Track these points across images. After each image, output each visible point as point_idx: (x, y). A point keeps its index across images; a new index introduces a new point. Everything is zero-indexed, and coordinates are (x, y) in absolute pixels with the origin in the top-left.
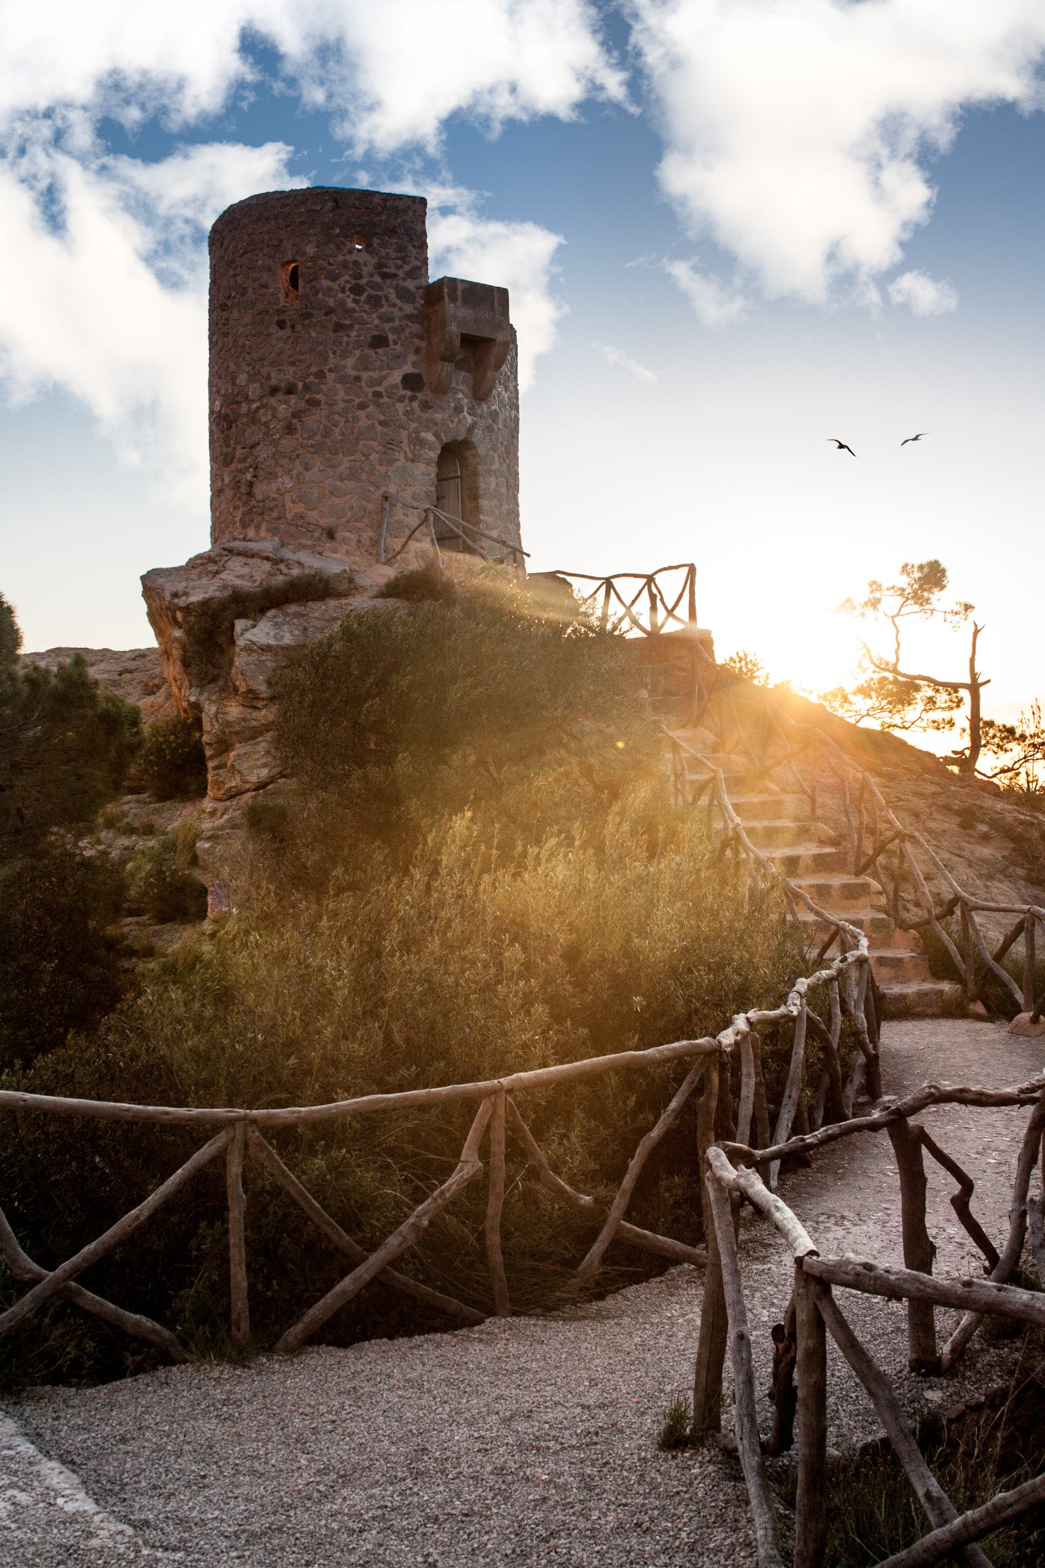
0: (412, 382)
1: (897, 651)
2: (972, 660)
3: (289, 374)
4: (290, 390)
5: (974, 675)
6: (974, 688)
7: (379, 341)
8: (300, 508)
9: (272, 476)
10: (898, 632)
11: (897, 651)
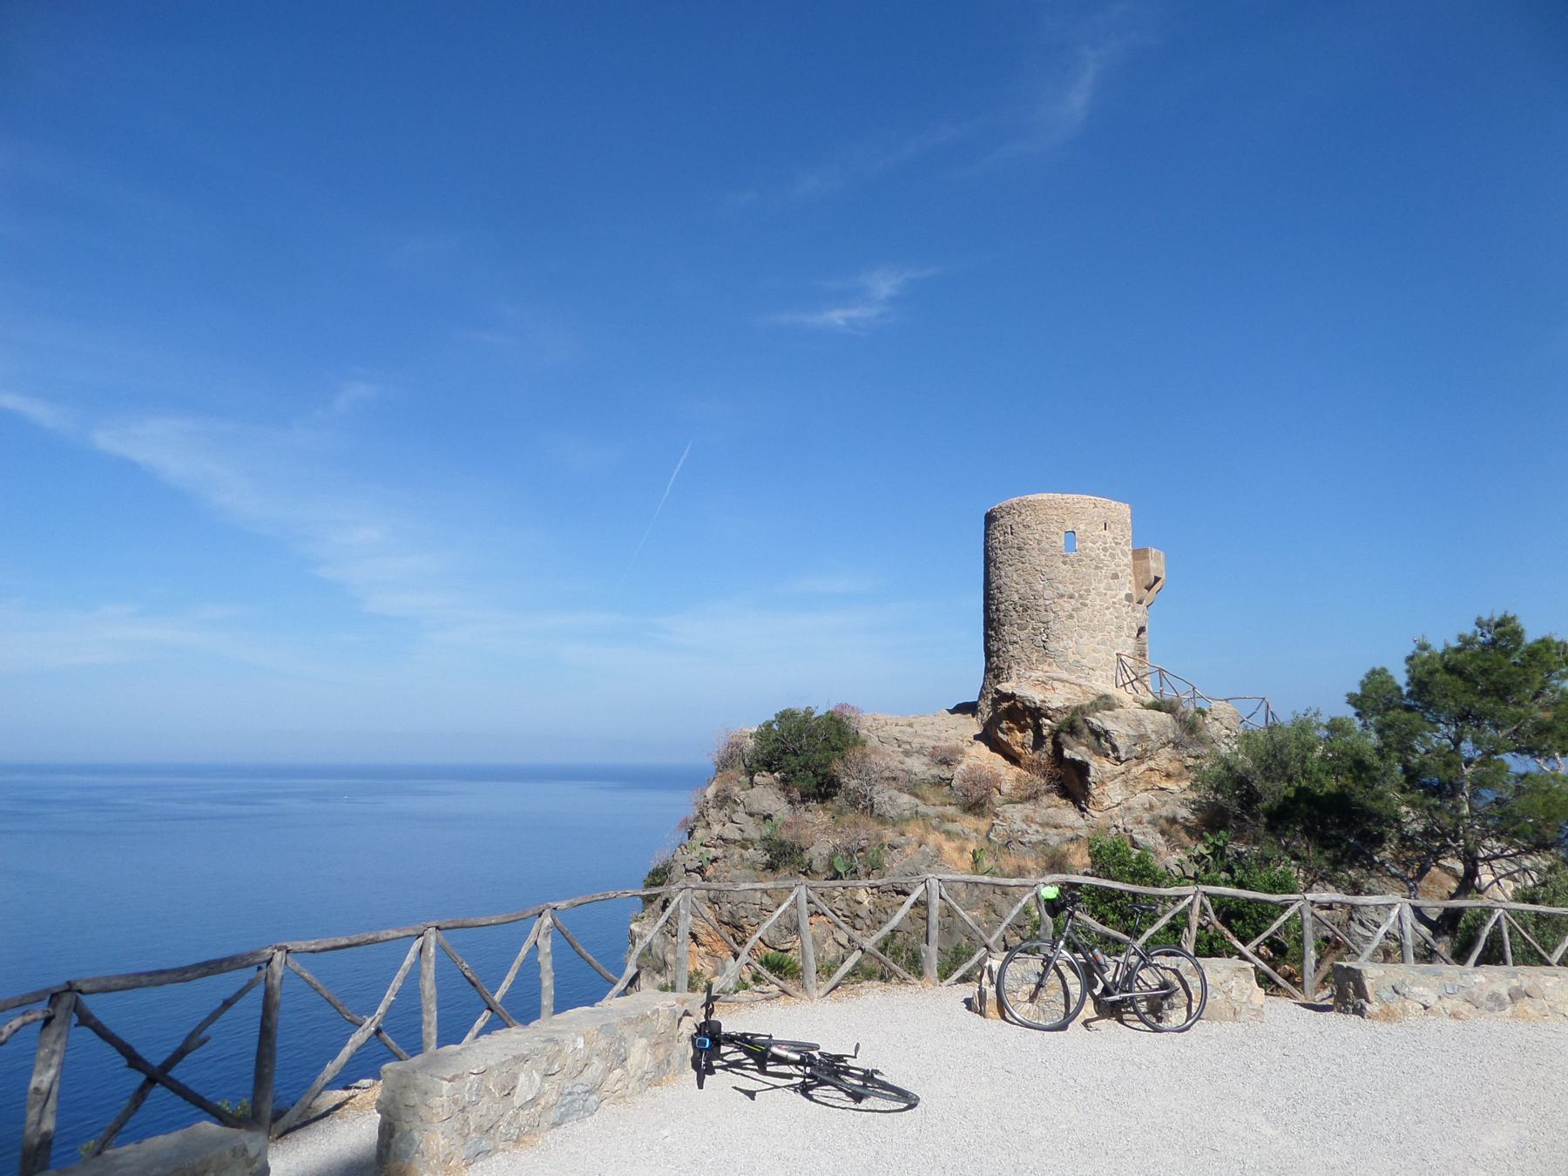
0: (1129, 597)
3: (1070, 589)
4: (1071, 597)
7: (1115, 576)
8: (1078, 657)
9: (1059, 638)
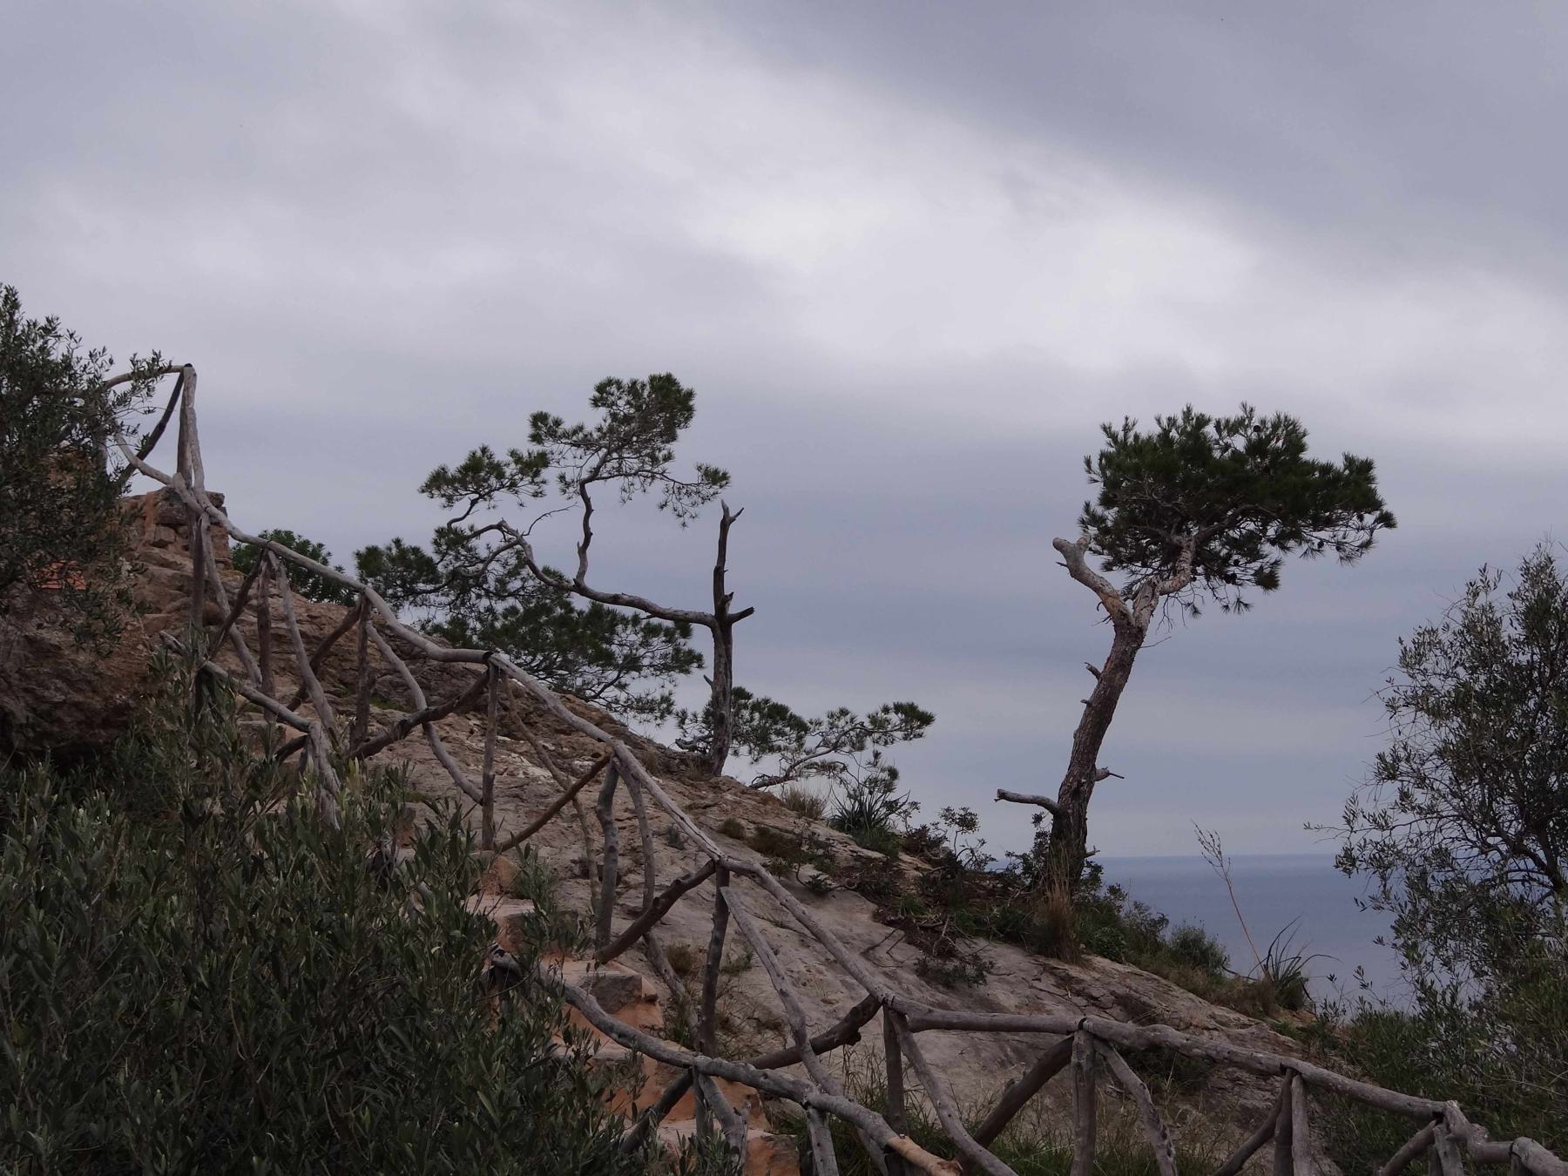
1: (582, 550)
2: (719, 574)
5: (722, 600)
6: (722, 624)
10: (589, 511)
11: (582, 550)
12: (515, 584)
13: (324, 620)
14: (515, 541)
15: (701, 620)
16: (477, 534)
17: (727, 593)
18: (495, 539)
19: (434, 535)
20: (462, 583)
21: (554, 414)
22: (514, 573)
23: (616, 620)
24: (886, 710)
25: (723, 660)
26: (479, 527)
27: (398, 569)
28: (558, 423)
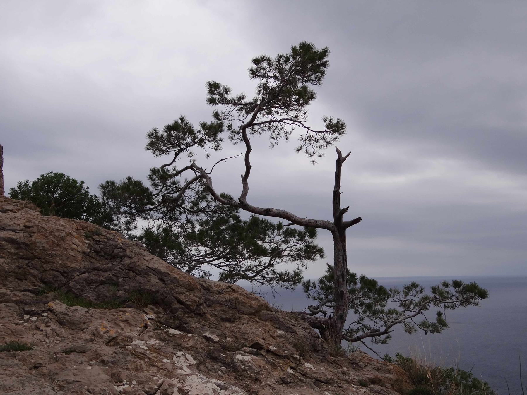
1: (245, 179)
2: (336, 195)
5: (338, 212)
6: (339, 229)
10: (249, 150)
11: (245, 179)
12: (203, 204)
13: (35, 229)
14: (203, 177)
15: (325, 226)
16: (178, 173)
17: (342, 207)
18: (190, 175)
19: (149, 173)
20: (171, 205)
21: (223, 83)
22: (202, 198)
23: (269, 227)
24: (446, 285)
25: (341, 254)
26: (179, 168)
27: (131, 195)
28: (227, 91)
